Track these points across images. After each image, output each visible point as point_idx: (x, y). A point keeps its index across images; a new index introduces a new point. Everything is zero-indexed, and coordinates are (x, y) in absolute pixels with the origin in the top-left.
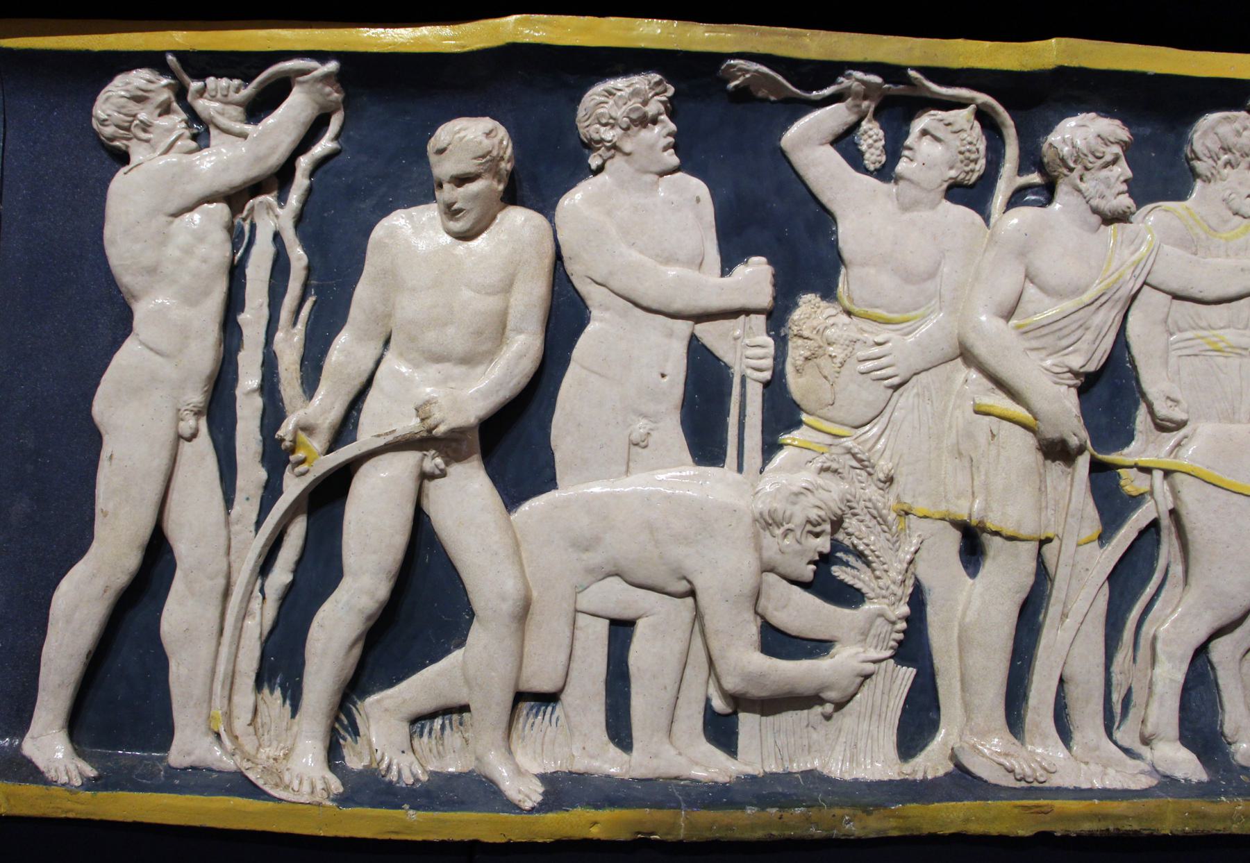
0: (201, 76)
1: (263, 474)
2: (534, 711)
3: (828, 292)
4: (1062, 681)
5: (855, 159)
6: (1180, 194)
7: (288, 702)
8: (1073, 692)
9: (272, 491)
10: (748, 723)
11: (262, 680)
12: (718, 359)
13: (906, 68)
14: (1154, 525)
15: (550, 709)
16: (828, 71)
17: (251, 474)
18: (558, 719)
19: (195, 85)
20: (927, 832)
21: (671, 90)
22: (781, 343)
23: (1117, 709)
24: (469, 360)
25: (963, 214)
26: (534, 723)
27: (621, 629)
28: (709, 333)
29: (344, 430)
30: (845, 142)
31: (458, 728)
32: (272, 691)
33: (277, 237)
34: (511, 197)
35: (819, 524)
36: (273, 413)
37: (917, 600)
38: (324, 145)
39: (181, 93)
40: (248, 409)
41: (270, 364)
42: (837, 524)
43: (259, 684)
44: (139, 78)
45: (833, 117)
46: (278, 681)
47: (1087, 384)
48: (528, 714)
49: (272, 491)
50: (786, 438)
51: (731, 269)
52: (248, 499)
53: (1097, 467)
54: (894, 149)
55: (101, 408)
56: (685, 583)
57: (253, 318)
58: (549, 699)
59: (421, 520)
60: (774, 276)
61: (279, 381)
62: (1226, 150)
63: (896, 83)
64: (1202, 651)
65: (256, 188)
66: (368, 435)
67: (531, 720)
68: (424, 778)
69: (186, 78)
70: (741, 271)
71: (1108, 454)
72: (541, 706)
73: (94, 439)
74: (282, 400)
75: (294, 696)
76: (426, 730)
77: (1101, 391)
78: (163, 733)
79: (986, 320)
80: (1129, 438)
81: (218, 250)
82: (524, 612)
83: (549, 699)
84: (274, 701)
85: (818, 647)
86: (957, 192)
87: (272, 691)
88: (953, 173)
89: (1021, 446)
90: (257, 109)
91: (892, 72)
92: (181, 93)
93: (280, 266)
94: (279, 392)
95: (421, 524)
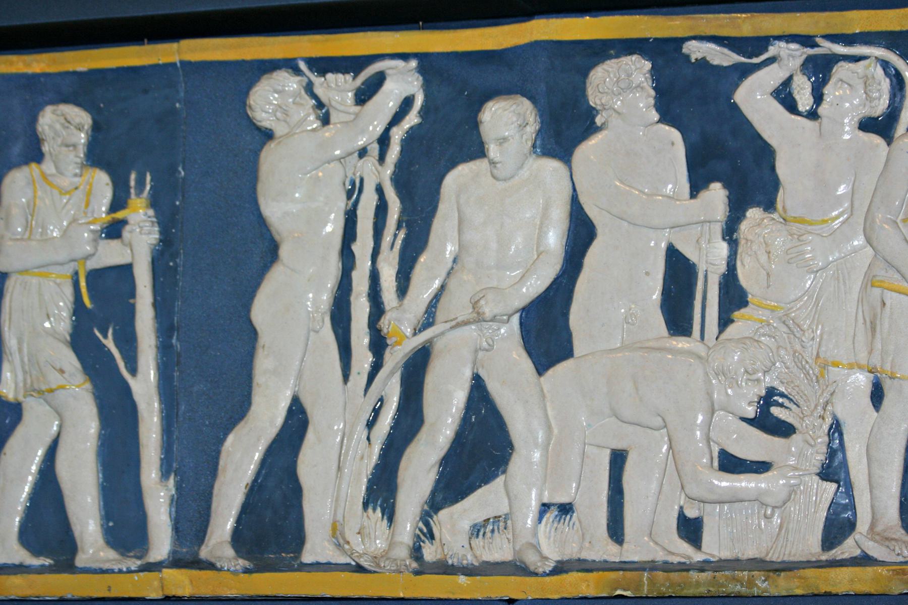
0: (322, 72)
1: (370, 358)
2: (558, 519)
3: (769, 205)
5: (791, 106)
7: (385, 517)
9: (376, 368)
12: (688, 260)
15: (568, 517)
16: (760, 44)
17: (362, 359)
18: (574, 524)
19: (317, 81)
20: (824, 591)
21: (648, 65)
26: (557, 528)
31: (503, 531)
32: (374, 510)
33: (380, 190)
35: (754, 373)
36: (377, 309)
39: (309, 88)
40: (360, 308)
41: (374, 278)
43: (365, 505)
45: (770, 77)
46: (379, 503)
48: (553, 521)
50: (736, 314)
51: (698, 192)
52: (359, 373)
54: (818, 98)
56: (660, 419)
57: (363, 247)
60: (728, 197)
61: (380, 290)
67: (555, 525)
68: (476, 564)
69: (313, 77)
70: (704, 195)
72: (562, 515)
73: (253, 334)
74: (383, 303)
75: (390, 514)
76: (481, 533)
78: (299, 540)
86: (868, 125)
87: (374, 510)
90: (363, 96)
91: (807, 41)
92: (309, 88)
93: (382, 209)
94: (381, 297)
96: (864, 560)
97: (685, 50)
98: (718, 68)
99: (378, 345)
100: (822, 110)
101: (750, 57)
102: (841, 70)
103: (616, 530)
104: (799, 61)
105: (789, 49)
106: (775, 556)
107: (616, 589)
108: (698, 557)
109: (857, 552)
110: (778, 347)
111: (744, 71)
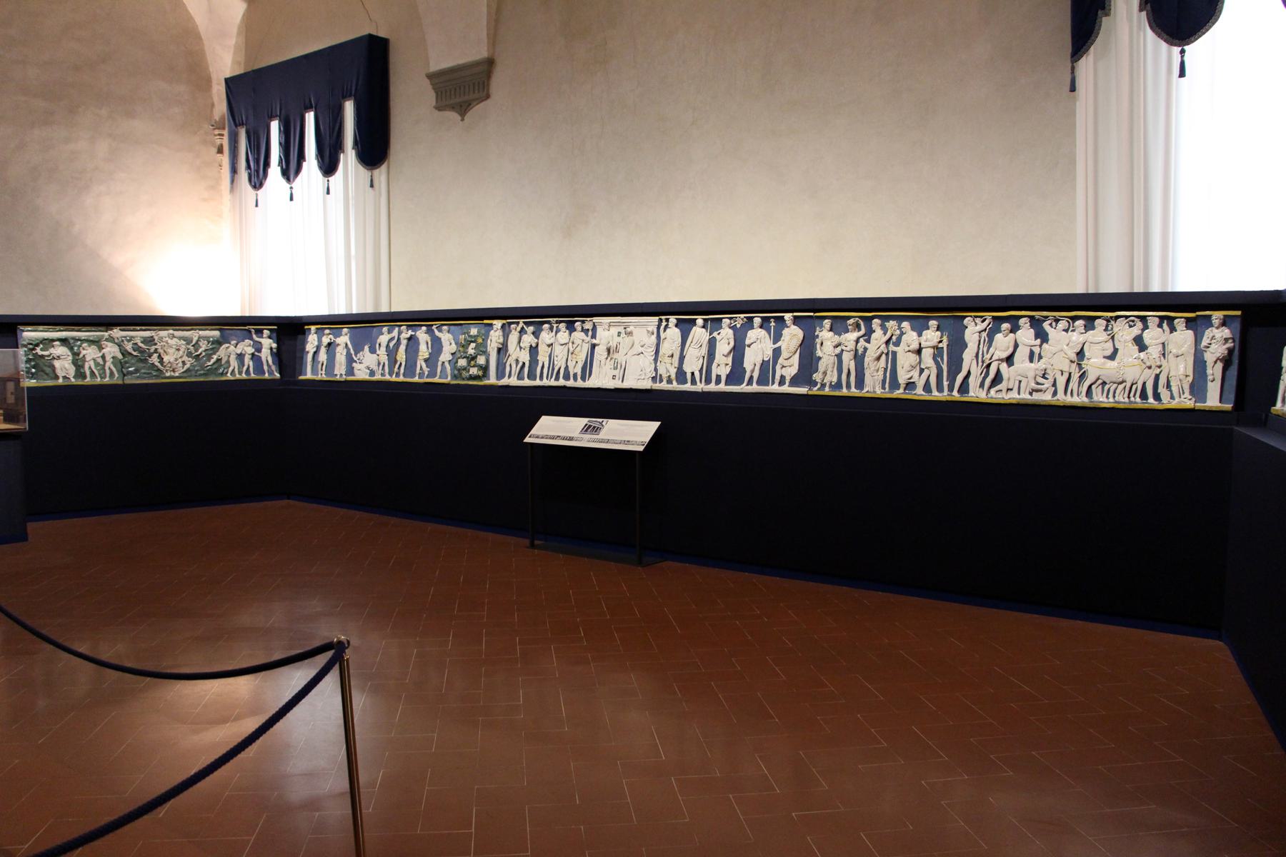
3: (1047, 343)
5: (1052, 327)
6: (1094, 330)
8: (1074, 391)
9: (982, 365)
10: (1034, 393)
11: (980, 387)
14: (1085, 372)
17: (980, 364)
22: (1041, 349)
24: (1004, 351)
25: (1064, 333)
27: (1020, 381)
28: (1032, 348)
29: (991, 359)
30: (1051, 325)
34: (1011, 332)
36: (983, 357)
37: (1055, 380)
38: (990, 326)
42: (1045, 370)
44: (969, 318)
45: (1049, 322)
47: (1078, 354)
49: (982, 365)
53: (1078, 364)
55: (963, 356)
57: (981, 346)
58: (1011, 390)
59: (998, 369)
64: (1090, 387)
65: (982, 331)
66: (994, 358)
73: (963, 360)
75: (983, 389)
77: (1080, 355)
78: (968, 393)
79: (1065, 346)
80: (1083, 360)
81: (978, 338)
82: (1009, 379)
83: (1011, 390)
84: (981, 390)
85: (1043, 384)
86: (1064, 330)
89: (1068, 361)
90: (983, 321)
91: (1055, 317)
93: (985, 340)
95: (998, 369)
96: (1058, 400)
99: (983, 362)
103: (1019, 394)
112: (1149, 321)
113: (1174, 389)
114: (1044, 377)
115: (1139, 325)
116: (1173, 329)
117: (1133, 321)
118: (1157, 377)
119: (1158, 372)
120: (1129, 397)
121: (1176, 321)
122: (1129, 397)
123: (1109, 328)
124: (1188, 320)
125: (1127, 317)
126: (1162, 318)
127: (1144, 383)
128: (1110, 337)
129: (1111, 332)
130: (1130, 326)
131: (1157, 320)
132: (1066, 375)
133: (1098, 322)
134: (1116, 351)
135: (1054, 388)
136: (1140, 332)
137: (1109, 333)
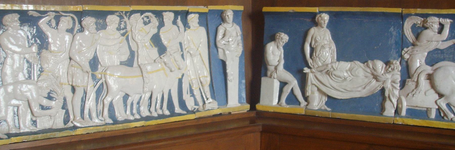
4: (89, 110)
5: (50, 26)
8: (92, 111)
13: (59, 11)
21: (19, 16)
23: (99, 113)
37: (65, 99)
54: (57, 24)
62: (112, 21)
63: (57, 13)
71: (94, 72)
86: (68, 31)
88: (67, 27)
96: (75, 128)
97: (28, 13)
98: (35, 17)
100: (58, 27)
101: (42, 15)
102: (62, 19)
104: (53, 17)
105: (52, 14)
106: (54, 127)
107: (23, 140)
108: (38, 130)
109: (72, 125)
110: (51, 81)
111: (40, 18)
112: (165, 17)
113: (197, 93)
114: (50, 98)
115: (155, 21)
116: (186, 25)
117: (148, 17)
118: (180, 82)
119: (180, 77)
120: (156, 110)
121: (190, 17)
122: (156, 110)
123: (122, 26)
124: (201, 14)
125: (142, 12)
126: (176, 13)
127: (170, 90)
128: (125, 37)
129: (124, 31)
130: (145, 23)
131: (172, 15)
132: (79, 94)
133: (110, 18)
134: (132, 54)
135: (64, 111)
136: (156, 31)
137: (122, 32)
